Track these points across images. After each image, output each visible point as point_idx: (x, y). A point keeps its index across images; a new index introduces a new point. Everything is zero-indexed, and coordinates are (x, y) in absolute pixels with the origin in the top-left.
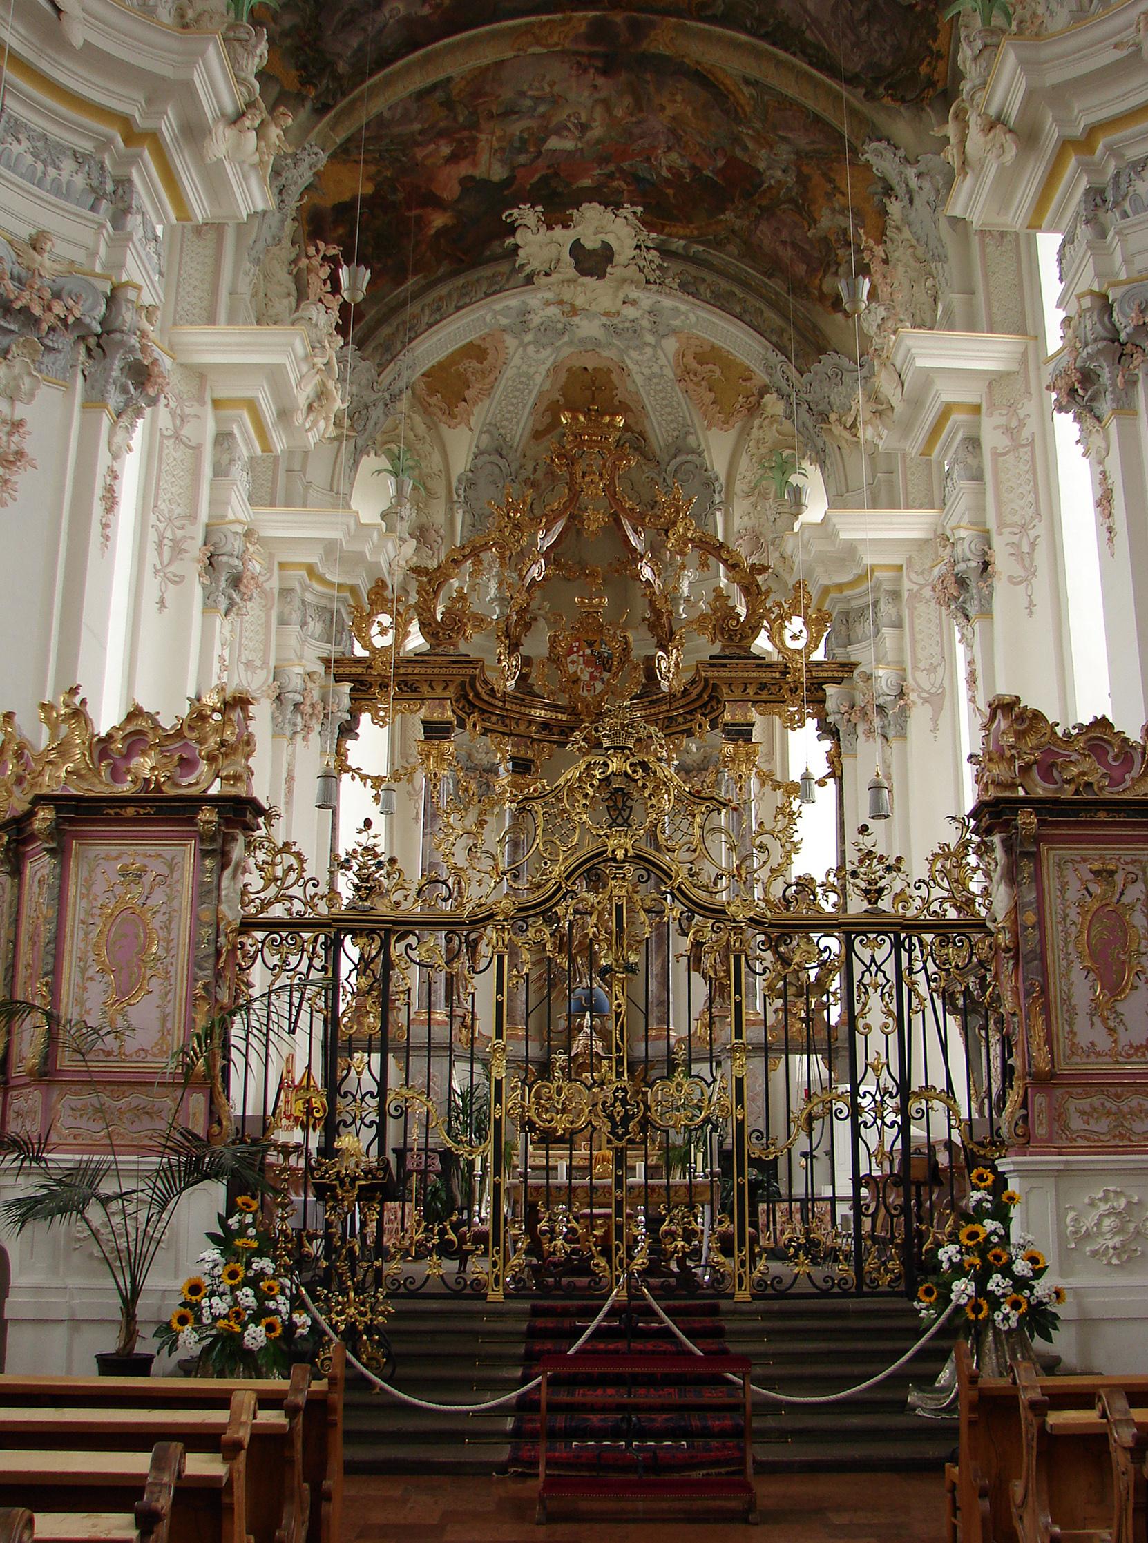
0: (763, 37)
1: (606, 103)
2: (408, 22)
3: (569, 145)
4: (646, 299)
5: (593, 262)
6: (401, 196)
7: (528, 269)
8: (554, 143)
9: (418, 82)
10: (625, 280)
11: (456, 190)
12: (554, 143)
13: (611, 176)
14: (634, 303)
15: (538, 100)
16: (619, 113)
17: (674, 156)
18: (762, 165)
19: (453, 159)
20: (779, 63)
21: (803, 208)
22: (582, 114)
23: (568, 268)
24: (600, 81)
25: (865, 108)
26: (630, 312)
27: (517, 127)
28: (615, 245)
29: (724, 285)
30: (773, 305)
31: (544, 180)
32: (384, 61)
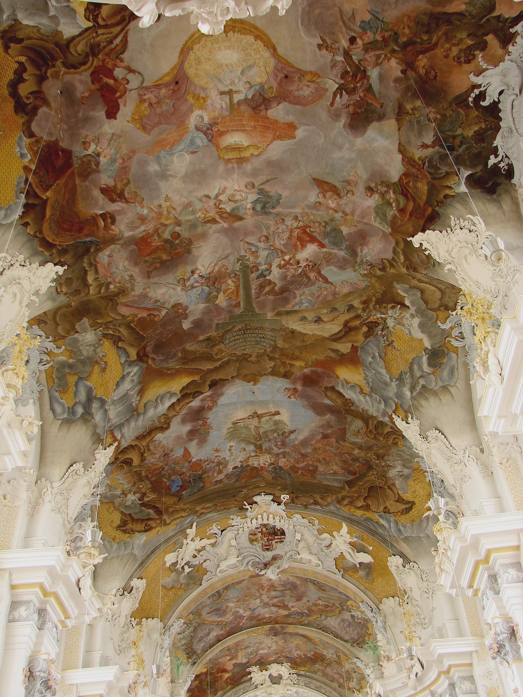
0: (320, 629)
1: (276, 642)
2: (217, 636)
3: (266, 651)
4: (294, 689)
5: (276, 680)
6: (215, 670)
7: (255, 684)
8: (261, 652)
9: (220, 648)
10: (287, 684)
11: (232, 667)
12: (261, 652)
13: (279, 657)
14: (290, 690)
15: (255, 644)
16: (280, 643)
17: (298, 652)
18: (325, 653)
19: (231, 659)
20: (325, 635)
21: (339, 663)
22: (268, 644)
23: (268, 682)
24: (274, 637)
25: (352, 649)
26: (290, 692)
27: (249, 650)
28: (282, 674)
29: (318, 684)
30: (335, 690)
31: (259, 660)
32: (211, 647)
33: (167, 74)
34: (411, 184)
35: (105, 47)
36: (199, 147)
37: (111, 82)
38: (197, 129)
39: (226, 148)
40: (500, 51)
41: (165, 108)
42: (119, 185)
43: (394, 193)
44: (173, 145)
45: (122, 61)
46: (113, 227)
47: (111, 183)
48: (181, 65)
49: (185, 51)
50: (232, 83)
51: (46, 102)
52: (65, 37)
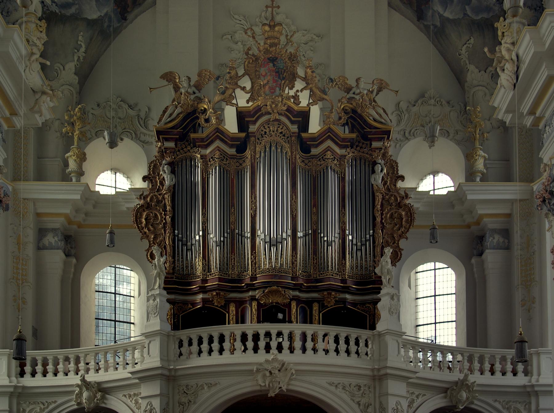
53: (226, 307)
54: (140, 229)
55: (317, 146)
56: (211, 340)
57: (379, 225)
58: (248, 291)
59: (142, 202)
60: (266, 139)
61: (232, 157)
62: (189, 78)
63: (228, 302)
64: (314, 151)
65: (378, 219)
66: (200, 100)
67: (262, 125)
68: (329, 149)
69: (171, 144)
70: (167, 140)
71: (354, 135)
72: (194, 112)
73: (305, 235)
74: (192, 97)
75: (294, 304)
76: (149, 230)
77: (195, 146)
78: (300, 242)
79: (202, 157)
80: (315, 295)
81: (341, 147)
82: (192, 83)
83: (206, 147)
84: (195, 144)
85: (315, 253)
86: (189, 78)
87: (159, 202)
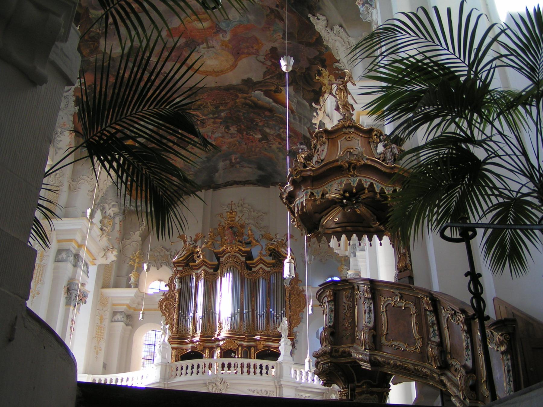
33: (243, 58)
34: (92, 46)
35: (275, 76)
36: (224, 22)
37: (273, 61)
38: (225, 32)
39: (207, 20)
40: (77, 94)
41: (245, 44)
42: (273, 17)
43: (99, 33)
44: (240, 26)
45: (267, 68)
46: (278, 3)
47: (277, 20)
48: (236, 60)
49: (234, 66)
50: (208, 52)
51: (309, 60)
52: (292, 87)
53: (204, 350)
54: (162, 311)
55: (255, 267)
56: (193, 367)
57: (288, 306)
58: (215, 342)
59: (164, 297)
60: (229, 264)
61: (211, 274)
62: (191, 237)
63: (205, 348)
64: (253, 269)
65: (288, 303)
66: (196, 247)
67: (227, 258)
68: (261, 268)
69: (181, 269)
70: (178, 266)
71: (274, 261)
72: (193, 253)
73: (248, 312)
74: (192, 246)
75: (240, 348)
76: (166, 311)
77: (193, 269)
78: (245, 316)
79: (196, 274)
80: (252, 343)
81: (268, 267)
82: (193, 239)
83: (198, 269)
84: (192, 268)
85: (253, 321)
86: (191, 237)
87: (172, 297)
